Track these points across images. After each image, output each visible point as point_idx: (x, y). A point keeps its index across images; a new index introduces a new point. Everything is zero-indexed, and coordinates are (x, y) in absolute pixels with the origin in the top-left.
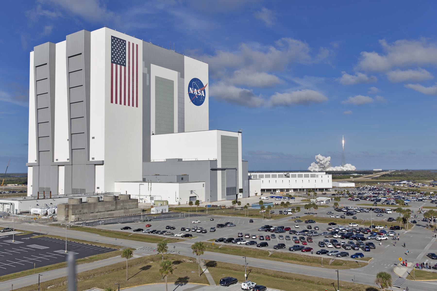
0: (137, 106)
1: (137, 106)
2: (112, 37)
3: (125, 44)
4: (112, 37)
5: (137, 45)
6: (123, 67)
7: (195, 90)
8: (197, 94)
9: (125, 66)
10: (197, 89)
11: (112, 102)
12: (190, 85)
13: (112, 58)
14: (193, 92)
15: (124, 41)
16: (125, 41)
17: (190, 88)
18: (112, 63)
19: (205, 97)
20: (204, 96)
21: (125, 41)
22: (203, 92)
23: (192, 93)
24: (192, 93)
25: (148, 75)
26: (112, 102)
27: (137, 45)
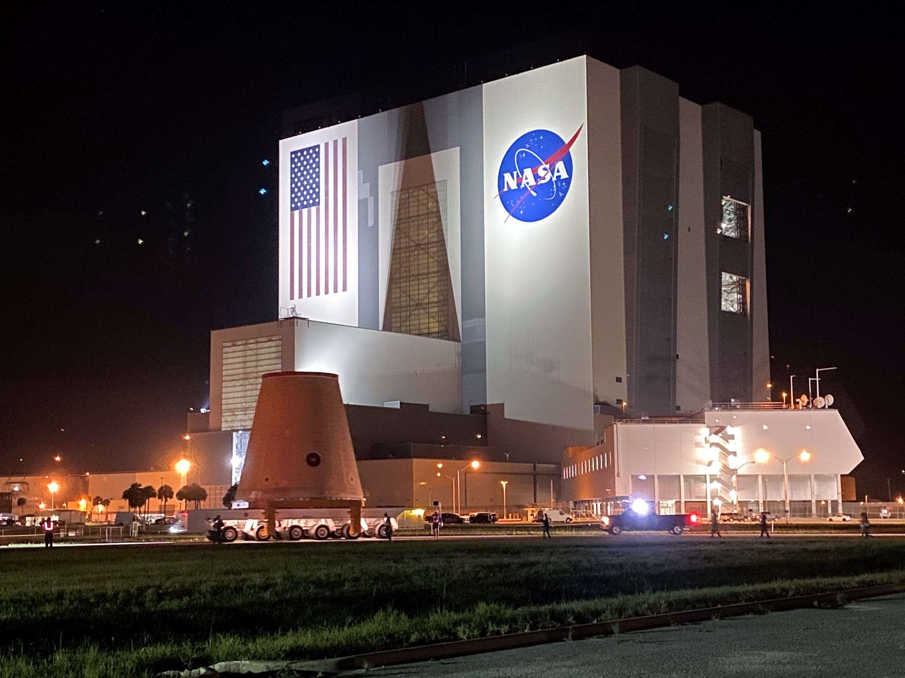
2: (292, 153)
3: (318, 154)
4: (292, 153)
6: (314, 209)
7: (528, 172)
8: (532, 182)
10: (534, 166)
14: (519, 184)
15: (314, 148)
16: (318, 146)
17: (507, 176)
18: (292, 209)
19: (568, 181)
20: (564, 175)
21: (318, 146)
22: (560, 165)
23: (513, 186)
24: (513, 186)
25: (371, 200)
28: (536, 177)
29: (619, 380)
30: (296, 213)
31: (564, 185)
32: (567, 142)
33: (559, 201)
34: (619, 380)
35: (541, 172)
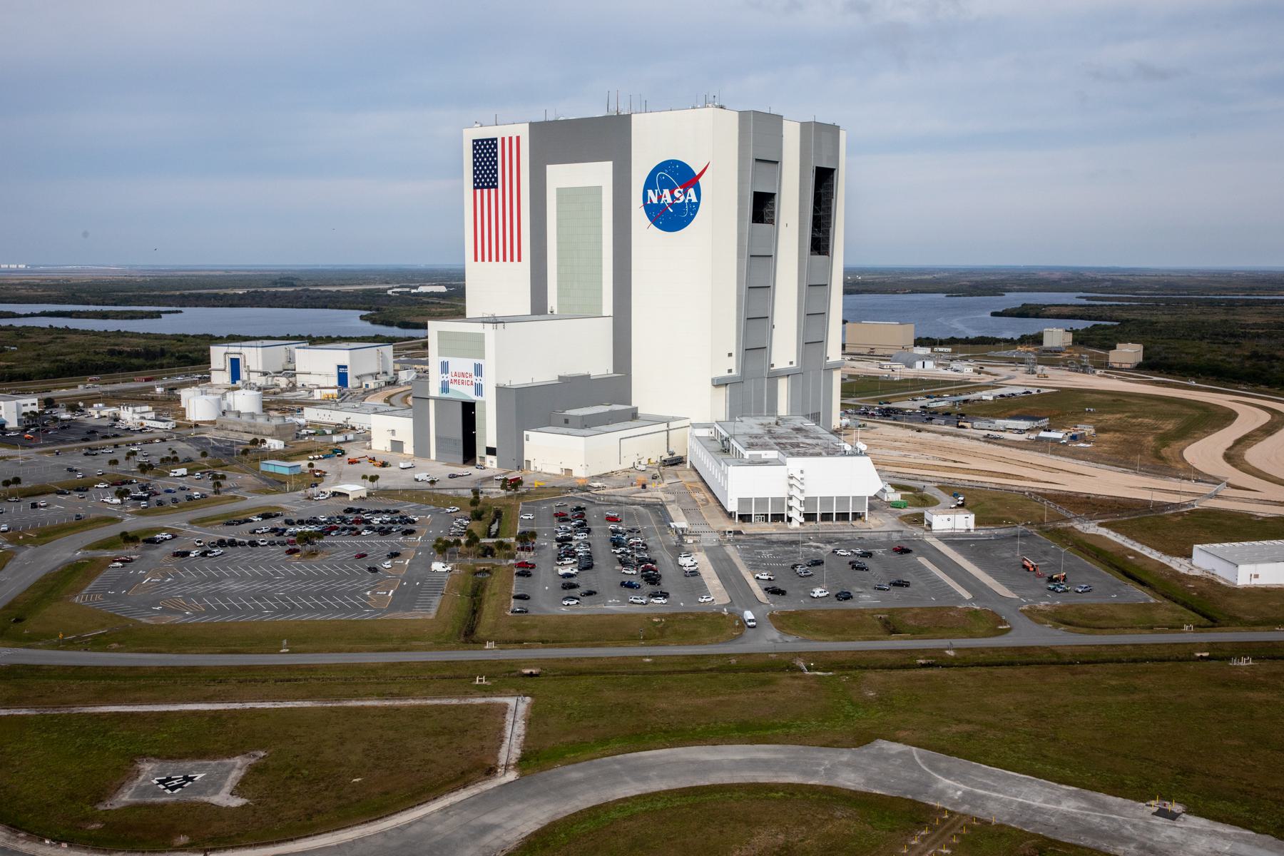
0: (519, 260)
1: (519, 260)
3: (496, 146)
5: (518, 138)
6: (493, 190)
7: (666, 192)
9: (496, 187)
11: (476, 260)
12: (650, 184)
13: (475, 181)
15: (493, 140)
17: (650, 192)
19: (697, 205)
20: (694, 200)
22: (691, 191)
23: (655, 201)
24: (655, 201)
26: (476, 260)
27: (518, 138)
28: (673, 197)
29: (730, 355)
30: (478, 191)
31: (694, 208)
32: (697, 173)
33: (689, 219)
34: (730, 355)
35: (677, 194)
